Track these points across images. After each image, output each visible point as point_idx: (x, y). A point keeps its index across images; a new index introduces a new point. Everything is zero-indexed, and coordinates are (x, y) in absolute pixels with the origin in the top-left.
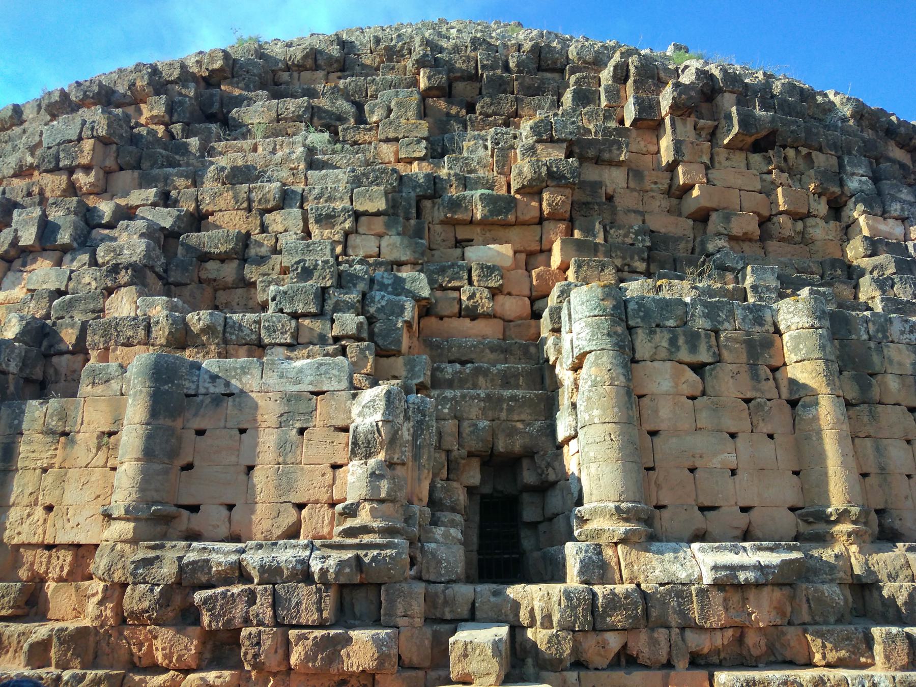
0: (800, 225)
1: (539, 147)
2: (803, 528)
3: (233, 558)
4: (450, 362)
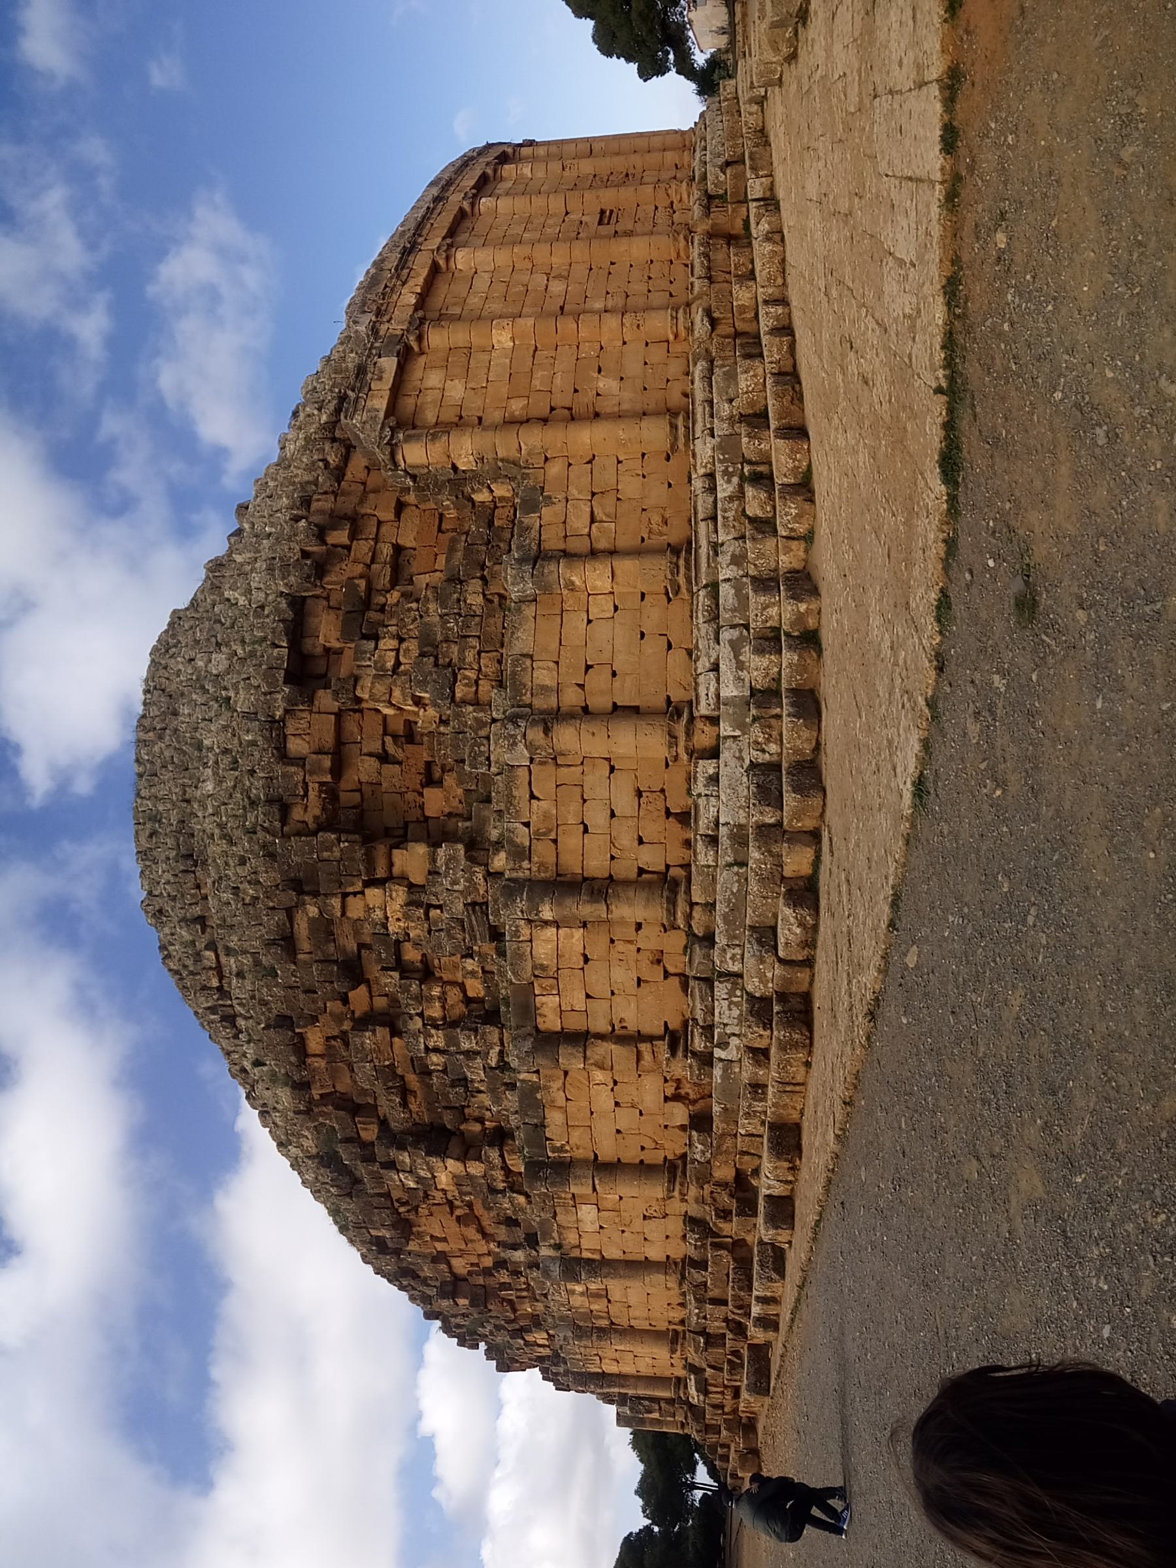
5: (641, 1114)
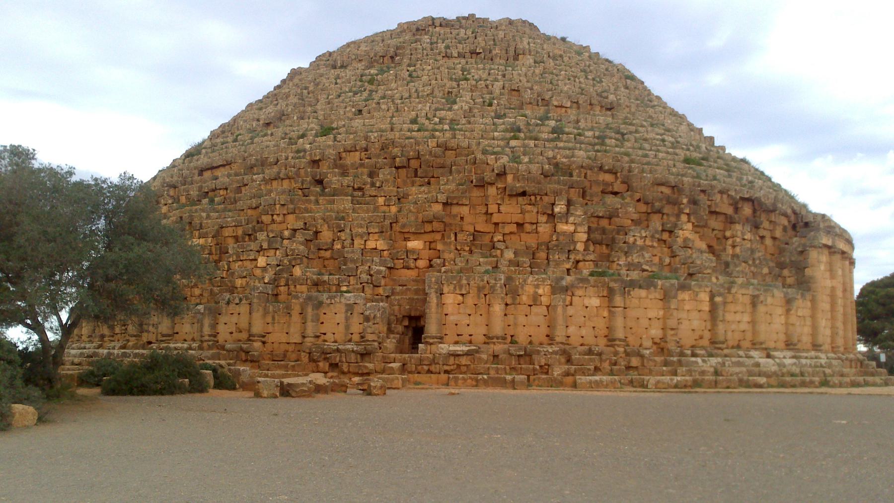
0: (534, 226)
2: (487, 341)
3: (336, 347)
5: (646, 328)
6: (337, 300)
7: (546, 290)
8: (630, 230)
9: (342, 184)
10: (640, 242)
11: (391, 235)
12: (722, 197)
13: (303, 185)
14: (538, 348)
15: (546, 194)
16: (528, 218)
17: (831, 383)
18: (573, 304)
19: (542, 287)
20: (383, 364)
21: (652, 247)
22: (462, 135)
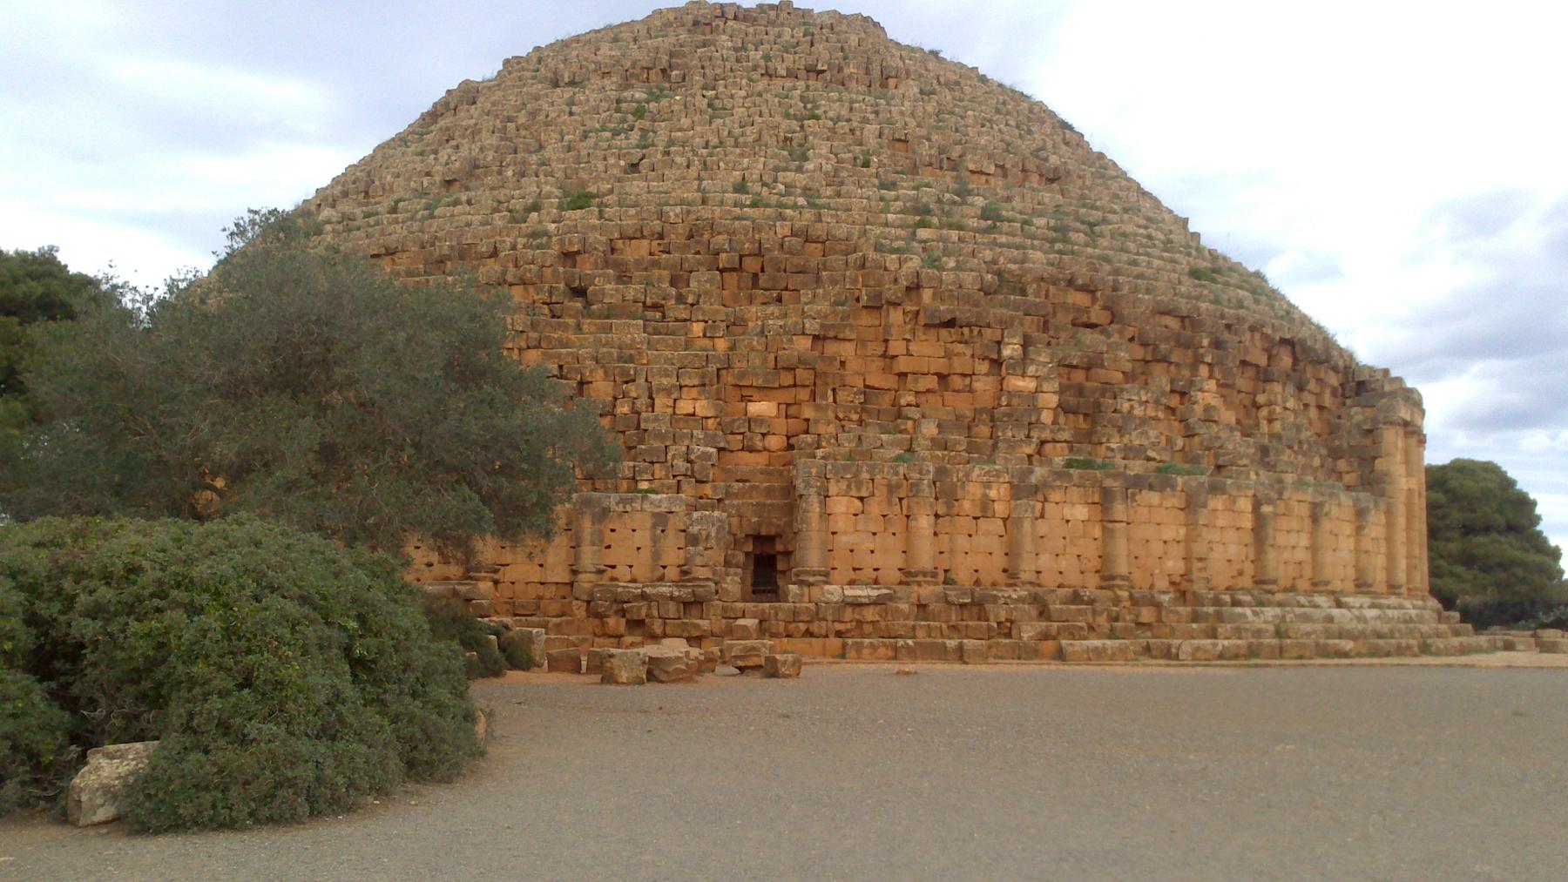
0: (968, 380)
1: (794, 337)
2: (904, 579)
3: (639, 591)
4: (737, 481)
6: (637, 505)
7: (1002, 490)
8: (1122, 390)
9: (623, 297)
10: (1138, 411)
11: (718, 392)
12: (1252, 337)
13: (551, 297)
14: (994, 592)
15: (988, 326)
16: (959, 365)
17: (1433, 649)
18: (1046, 516)
19: (994, 486)
20: (724, 621)
21: (1156, 419)
22: (832, 216)
